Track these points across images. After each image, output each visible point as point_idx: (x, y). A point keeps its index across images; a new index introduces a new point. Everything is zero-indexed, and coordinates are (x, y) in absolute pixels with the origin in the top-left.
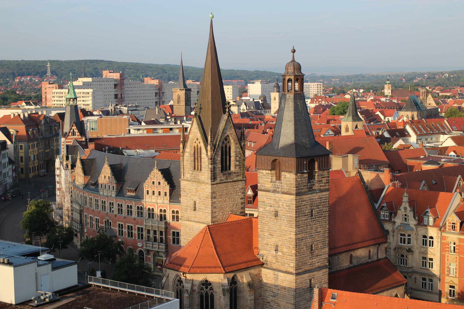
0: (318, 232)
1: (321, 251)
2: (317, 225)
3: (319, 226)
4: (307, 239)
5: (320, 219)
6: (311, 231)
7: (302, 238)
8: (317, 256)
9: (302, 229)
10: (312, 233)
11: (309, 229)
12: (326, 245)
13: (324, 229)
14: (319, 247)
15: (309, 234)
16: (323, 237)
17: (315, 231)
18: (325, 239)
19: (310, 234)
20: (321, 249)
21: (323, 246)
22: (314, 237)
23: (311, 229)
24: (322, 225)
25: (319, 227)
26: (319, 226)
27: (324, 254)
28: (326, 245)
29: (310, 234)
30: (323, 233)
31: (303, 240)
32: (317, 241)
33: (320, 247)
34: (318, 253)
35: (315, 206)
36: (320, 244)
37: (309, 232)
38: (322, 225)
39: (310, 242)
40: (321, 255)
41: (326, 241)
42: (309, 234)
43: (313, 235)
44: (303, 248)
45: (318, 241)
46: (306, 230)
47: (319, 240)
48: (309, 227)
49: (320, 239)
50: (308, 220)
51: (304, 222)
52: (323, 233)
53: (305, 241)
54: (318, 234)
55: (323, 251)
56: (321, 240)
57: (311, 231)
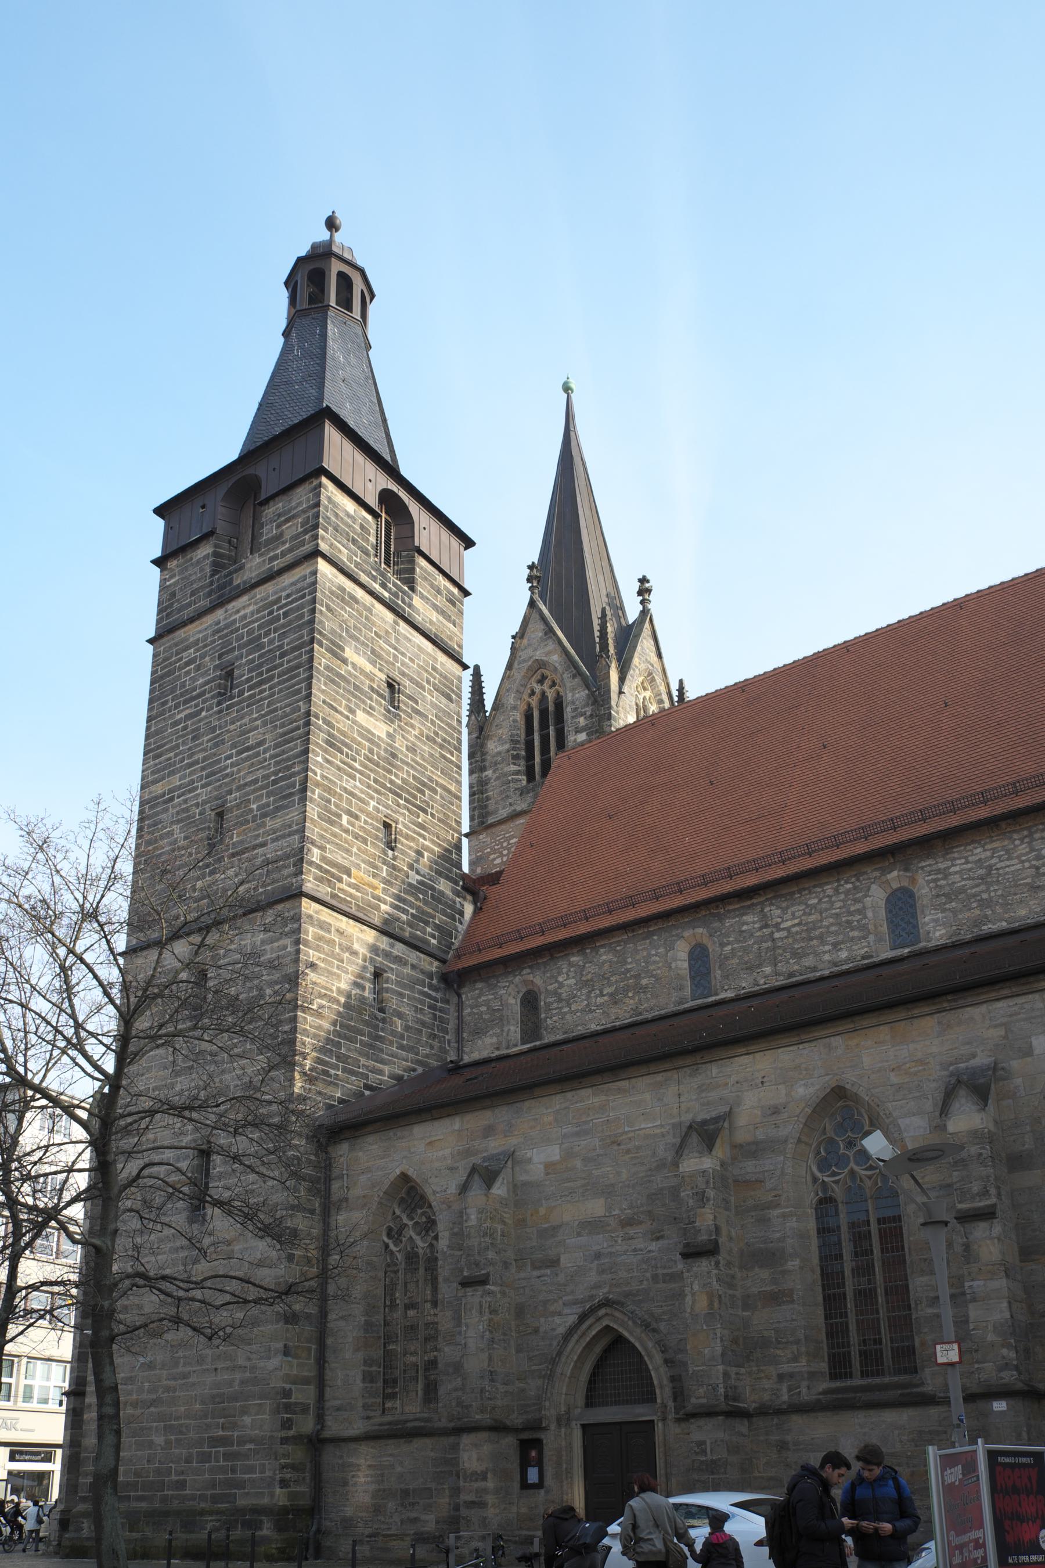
0: (248, 749)
1: (264, 825)
2: (246, 720)
3: (256, 719)
4: (196, 788)
5: (261, 692)
6: (215, 755)
7: (171, 791)
8: (242, 852)
9: (170, 759)
10: (219, 761)
11: (205, 750)
12: (292, 794)
13: (283, 726)
14: (251, 810)
15: (203, 769)
16: (277, 763)
17: (234, 746)
18: (288, 768)
19: (211, 765)
20: (264, 815)
21: (275, 801)
22: (227, 775)
23: (216, 745)
24: (276, 710)
25: (259, 722)
26: (256, 719)
27: (273, 840)
28: (292, 794)
29: (211, 765)
30: (276, 746)
31: (172, 799)
32: (239, 788)
33: (259, 809)
34: (242, 842)
35: (240, 647)
36: (259, 798)
37: (205, 759)
38: (276, 710)
39: (204, 803)
40: (263, 845)
41: (294, 775)
42: (203, 769)
43: (226, 767)
44: (170, 834)
45: (246, 784)
46: (190, 756)
47: (256, 781)
48: (206, 739)
49: (260, 774)
50: (204, 714)
51: (185, 728)
52: (276, 746)
53: (180, 805)
54: (249, 758)
55: (270, 823)
56: (266, 777)
57: (215, 755)
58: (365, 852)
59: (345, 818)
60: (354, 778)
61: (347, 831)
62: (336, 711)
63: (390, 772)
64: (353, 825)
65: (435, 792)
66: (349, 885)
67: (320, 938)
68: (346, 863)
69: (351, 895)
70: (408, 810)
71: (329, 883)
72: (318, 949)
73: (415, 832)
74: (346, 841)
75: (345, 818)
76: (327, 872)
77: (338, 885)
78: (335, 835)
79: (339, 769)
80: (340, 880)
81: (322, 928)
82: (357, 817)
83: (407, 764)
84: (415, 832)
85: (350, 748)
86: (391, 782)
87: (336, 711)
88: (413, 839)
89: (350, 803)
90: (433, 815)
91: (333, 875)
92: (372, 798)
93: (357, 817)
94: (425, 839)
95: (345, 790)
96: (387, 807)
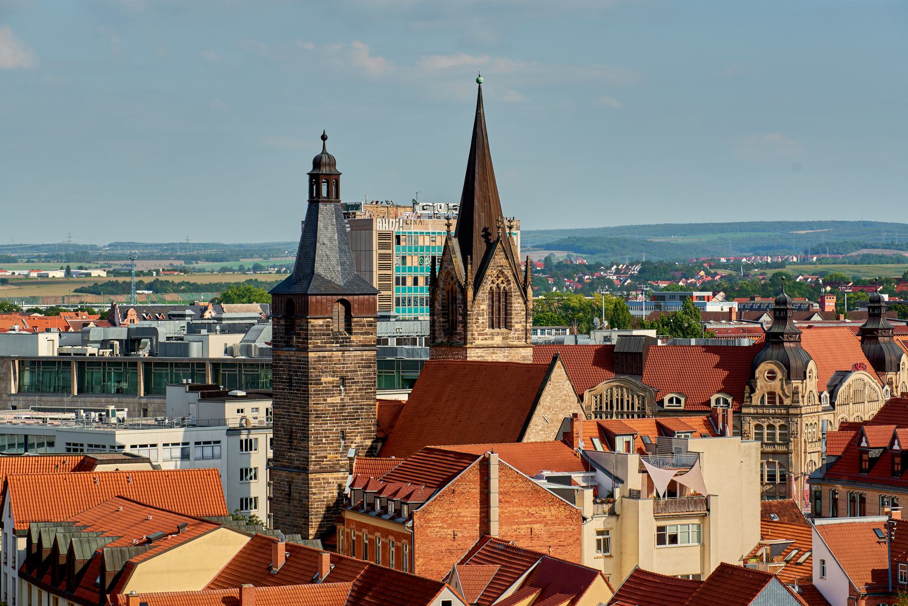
58: (333, 447)
59: (324, 439)
60: (327, 424)
61: (325, 444)
62: (319, 404)
63: (342, 413)
64: (327, 440)
65: (363, 409)
66: (327, 461)
67: (316, 484)
68: (325, 455)
69: (327, 465)
70: (351, 422)
71: (319, 464)
72: (315, 488)
73: (354, 429)
74: (325, 447)
75: (324, 439)
76: (318, 461)
77: (322, 463)
78: (320, 447)
79: (321, 424)
80: (323, 461)
81: (316, 480)
82: (329, 437)
83: (350, 405)
84: (354, 429)
85: (325, 414)
86: (343, 416)
87: (319, 404)
88: (353, 432)
89: (326, 433)
90: (362, 419)
91: (320, 461)
92: (335, 427)
93: (329, 437)
94: (358, 429)
95: (324, 430)
96: (342, 426)
